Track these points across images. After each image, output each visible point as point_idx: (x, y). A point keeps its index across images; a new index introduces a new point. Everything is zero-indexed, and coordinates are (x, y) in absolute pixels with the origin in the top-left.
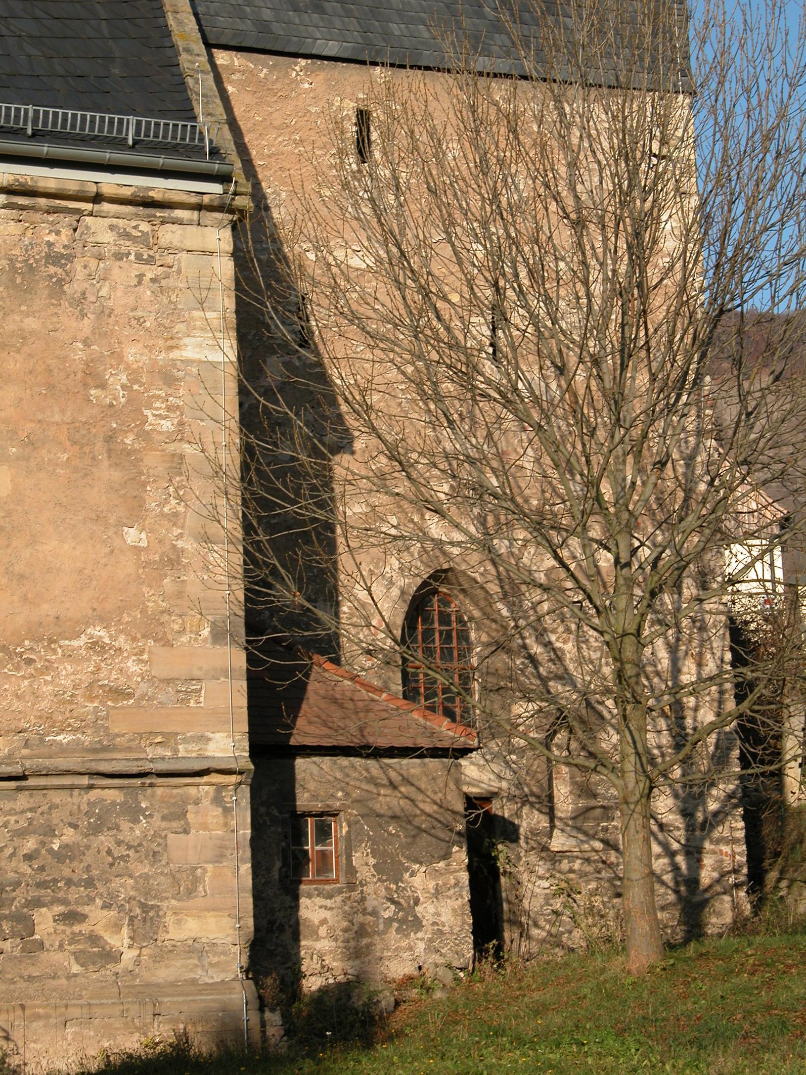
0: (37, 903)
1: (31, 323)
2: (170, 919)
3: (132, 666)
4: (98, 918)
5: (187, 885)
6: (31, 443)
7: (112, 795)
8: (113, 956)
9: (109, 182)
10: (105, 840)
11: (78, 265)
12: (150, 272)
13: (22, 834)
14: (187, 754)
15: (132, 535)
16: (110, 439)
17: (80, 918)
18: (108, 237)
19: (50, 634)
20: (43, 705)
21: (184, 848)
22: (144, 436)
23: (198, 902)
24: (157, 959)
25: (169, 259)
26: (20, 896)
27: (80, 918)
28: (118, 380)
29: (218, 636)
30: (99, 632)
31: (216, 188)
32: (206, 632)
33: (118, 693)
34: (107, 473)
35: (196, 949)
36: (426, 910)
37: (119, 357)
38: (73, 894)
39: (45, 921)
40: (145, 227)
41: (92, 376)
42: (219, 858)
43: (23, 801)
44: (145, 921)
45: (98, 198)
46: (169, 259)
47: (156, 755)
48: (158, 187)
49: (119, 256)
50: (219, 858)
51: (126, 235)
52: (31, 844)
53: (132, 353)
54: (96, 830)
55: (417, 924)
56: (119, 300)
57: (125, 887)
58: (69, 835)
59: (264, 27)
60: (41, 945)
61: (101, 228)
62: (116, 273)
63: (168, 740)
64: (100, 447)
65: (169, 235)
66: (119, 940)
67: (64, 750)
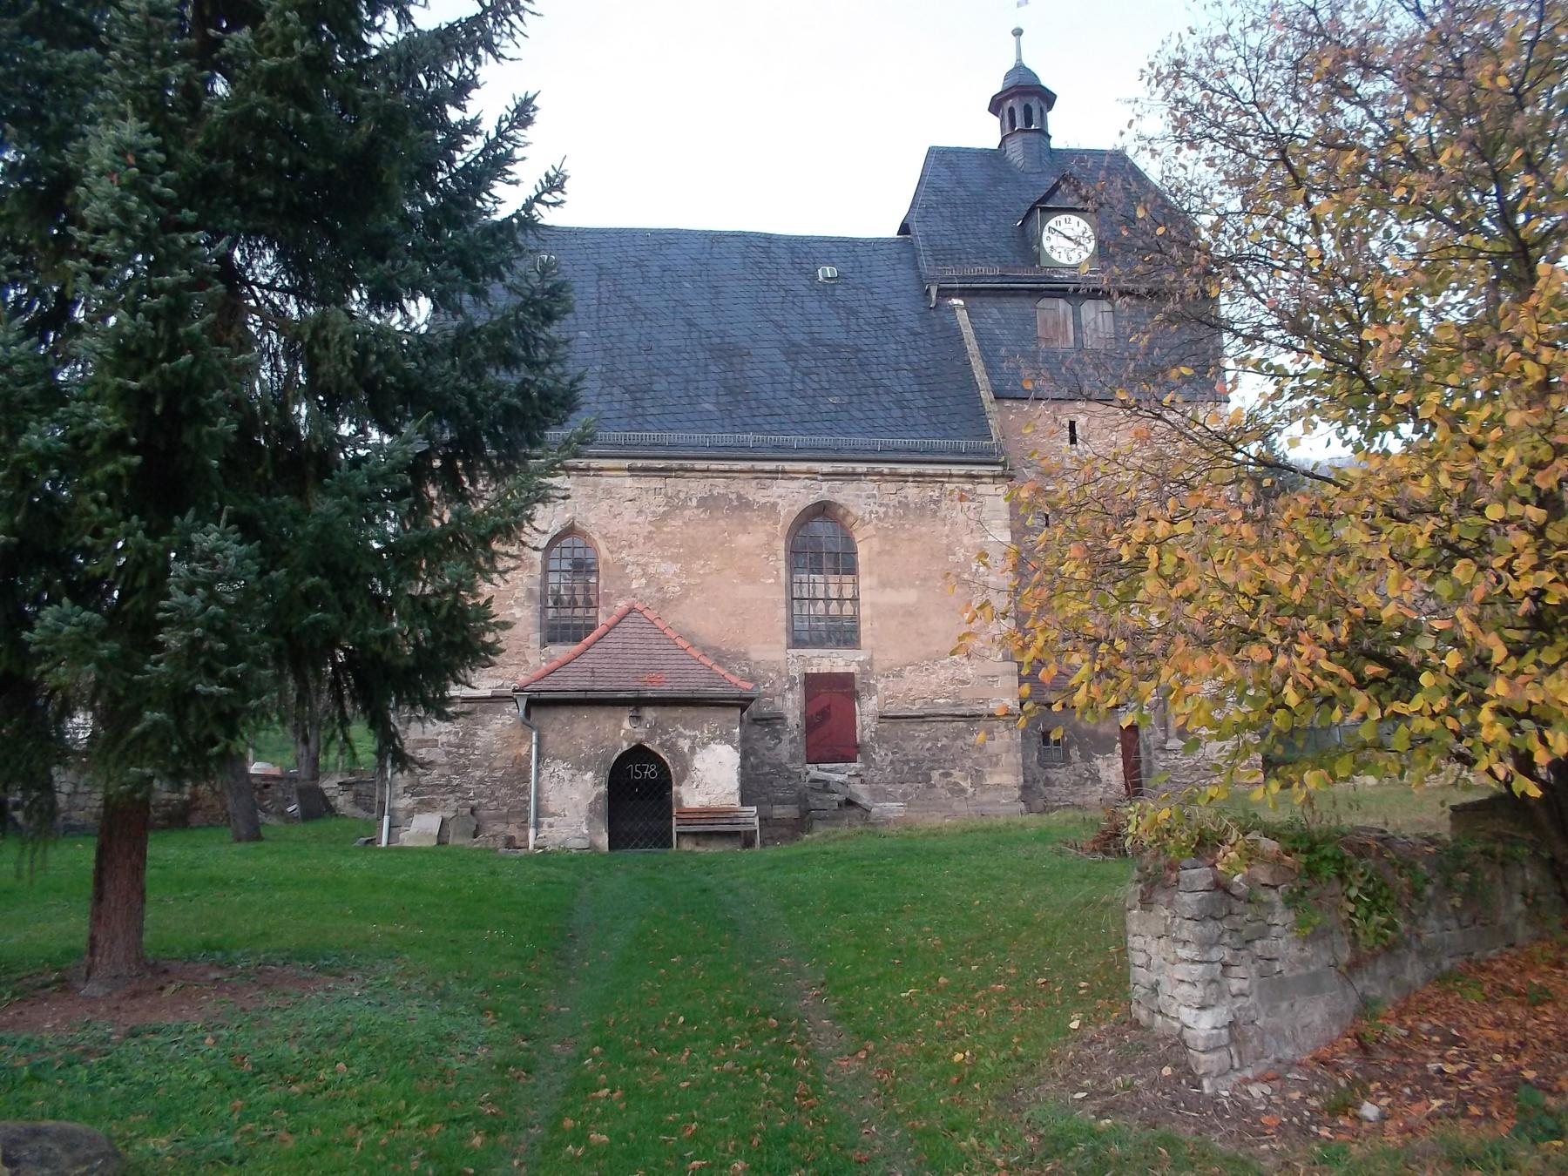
0: (932, 769)
1: (924, 529)
3: (969, 671)
4: (957, 775)
5: (994, 760)
6: (925, 579)
7: (962, 725)
8: (963, 791)
9: (955, 469)
10: (960, 743)
13: (926, 740)
14: (994, 707)
21: (994, 746)
23: (999, 769)
24: (983, 792)
26: (925, 766)
27: (949, 775)
28: (960, 552)
31: (1000, 468)
33: (964, 682)
35: (999, 787)
36: (1103, 774)
37: (960, 541)
39: (936, 775)
41: (950, 550)
44: (977, 777)
45: (951, 475)
47: (978, 709)
48: (976, 470)
50: (1008, 751)
53: (966, 540)
54: (955, 739)
55: (1099, 780)
56: (961, 518)
57: (968, 763)
58: (945, 741)
63: (985, 701)
65: (981, 489)
66: (966, 784)
67: (941, 705)
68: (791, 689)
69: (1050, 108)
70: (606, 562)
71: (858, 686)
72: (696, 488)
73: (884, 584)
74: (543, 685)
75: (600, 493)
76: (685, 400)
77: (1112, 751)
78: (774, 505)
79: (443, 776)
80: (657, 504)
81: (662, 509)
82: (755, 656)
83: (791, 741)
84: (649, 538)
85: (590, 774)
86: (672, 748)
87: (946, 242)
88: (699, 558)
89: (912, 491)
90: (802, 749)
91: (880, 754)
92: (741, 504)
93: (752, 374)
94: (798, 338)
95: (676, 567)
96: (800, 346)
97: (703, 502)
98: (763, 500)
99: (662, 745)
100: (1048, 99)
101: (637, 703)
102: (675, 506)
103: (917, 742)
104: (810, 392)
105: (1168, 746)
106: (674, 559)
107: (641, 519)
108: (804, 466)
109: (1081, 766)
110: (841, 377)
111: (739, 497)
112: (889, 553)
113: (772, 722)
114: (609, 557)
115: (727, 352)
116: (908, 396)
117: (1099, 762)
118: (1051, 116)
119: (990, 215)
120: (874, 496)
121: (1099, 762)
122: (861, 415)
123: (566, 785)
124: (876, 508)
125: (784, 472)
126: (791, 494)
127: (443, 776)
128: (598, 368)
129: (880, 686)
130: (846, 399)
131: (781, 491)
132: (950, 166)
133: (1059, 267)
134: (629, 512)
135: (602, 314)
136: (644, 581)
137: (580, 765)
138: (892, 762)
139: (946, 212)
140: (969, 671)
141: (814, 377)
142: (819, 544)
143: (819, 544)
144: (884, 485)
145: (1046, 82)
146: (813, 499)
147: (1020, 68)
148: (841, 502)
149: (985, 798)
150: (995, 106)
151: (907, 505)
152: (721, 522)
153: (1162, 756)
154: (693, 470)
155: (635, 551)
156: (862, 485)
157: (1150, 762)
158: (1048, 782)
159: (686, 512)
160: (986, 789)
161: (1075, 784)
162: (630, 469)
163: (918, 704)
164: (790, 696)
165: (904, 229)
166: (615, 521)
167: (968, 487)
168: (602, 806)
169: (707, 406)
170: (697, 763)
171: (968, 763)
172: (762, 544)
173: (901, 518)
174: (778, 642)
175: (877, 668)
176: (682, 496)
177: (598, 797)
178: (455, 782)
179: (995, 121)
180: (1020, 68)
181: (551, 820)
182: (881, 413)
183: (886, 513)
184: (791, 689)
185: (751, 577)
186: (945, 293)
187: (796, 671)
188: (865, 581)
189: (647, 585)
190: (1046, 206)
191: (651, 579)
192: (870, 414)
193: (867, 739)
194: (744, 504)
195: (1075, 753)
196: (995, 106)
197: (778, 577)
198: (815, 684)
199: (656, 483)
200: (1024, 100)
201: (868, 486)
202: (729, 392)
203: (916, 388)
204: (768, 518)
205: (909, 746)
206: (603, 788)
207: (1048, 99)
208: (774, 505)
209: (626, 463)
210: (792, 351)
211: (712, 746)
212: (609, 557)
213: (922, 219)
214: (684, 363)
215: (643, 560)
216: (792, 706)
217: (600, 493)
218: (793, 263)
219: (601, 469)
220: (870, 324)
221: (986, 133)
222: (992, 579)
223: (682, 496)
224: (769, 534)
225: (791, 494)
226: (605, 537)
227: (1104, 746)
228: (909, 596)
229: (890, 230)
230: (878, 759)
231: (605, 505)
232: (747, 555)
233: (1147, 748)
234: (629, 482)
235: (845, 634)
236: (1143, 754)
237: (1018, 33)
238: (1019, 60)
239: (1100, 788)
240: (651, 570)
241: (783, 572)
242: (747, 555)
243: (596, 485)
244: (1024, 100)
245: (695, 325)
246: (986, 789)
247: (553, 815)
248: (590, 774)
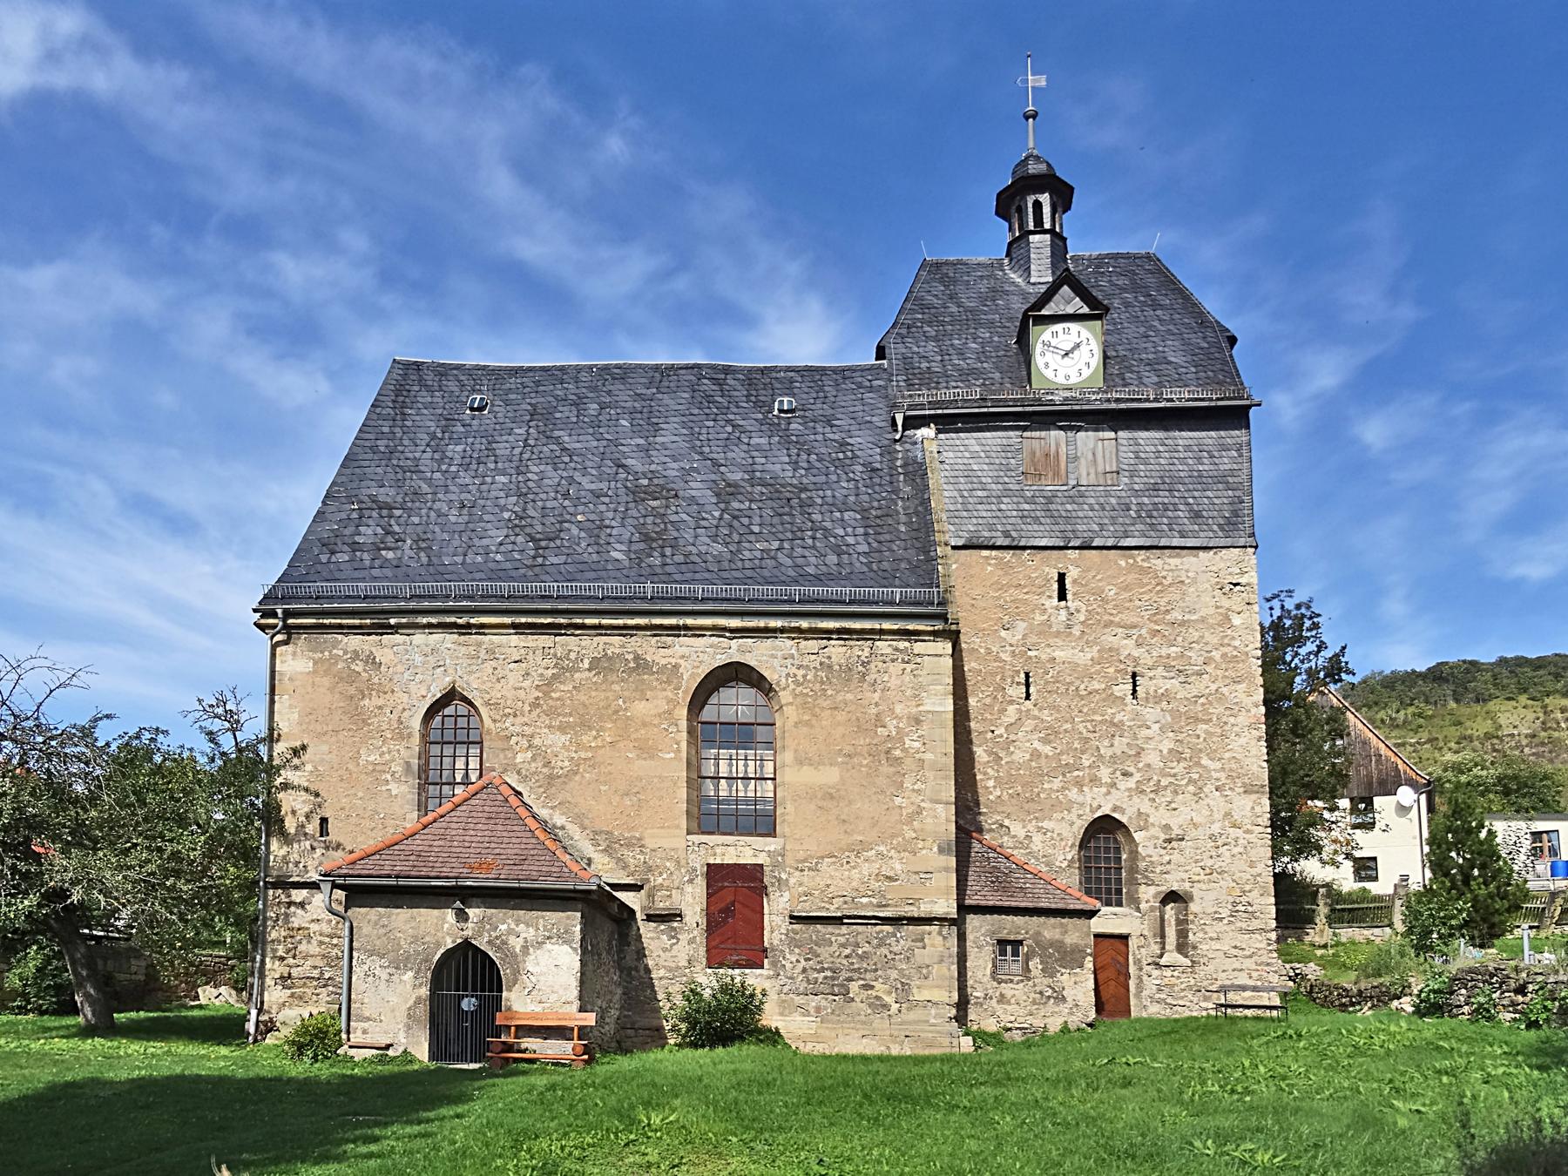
0: (850, 979)
1: (849, 696)
2: (915, 990)
3: (898, 866)
4: (880, 988)
5: (924, 972)
8: (886, 1007)
10: (884, 950)
11: (872, 665)
12: (909, 667)
13: (844, 946)
14: (924, 910)
15: (898, 801)
16: (887, 752)
17: (872, 987)
18: (889, 651)
19: (859, 849)
20: (854, 884)
21: (921, 956)
22: (904, 750)
23: (929, 982)
24: (909, 1009)
25: (919, 660)
26: (845, 975)
27: (872, 987)
28: (892, 725)
29: (941, 850)
30: (882, 848)
32: (935, 849)
33: (889, 878)
34: (886, 769)
37: (892, 710)
38: (868, 976)
39: (854, 987)
40: (907, 644)
41: (879, 721)
42: (941, 961)
43: (844, 929)
46: (919, 660)
49: (893, 661)
51: (896, 649)
52: (847, 952)
53: (898, 709)
54: (879, 946)
55: (1064, 999)
56: (894, 683)
58: (867, 948)
59: (1006, 534)
60: (853, 1000)
61: (883, 646)
62: (891, 669)
63: (914, 902)
64: (883, 756)
65: (919, 647)
66: (889, 999)
67: (864, 906)
68: (691, 881)
69: (1067, 208)
70: (489, 732)
71: (766, 880)
72: (591, 645)
73: (800, 762)
74: (367, 867)
75: (483, 654)
77: (1081, 966)
78: (676, 667)
79: (315, 967)
80: (542, 668)
81: (550, 672)
82: (650, 843)
83: (691, 941)
84: (535, 705)
85: (410, 974)
86: (502, 946)
88: (590, 728)
89: (837, 651)
90: (702, 951)
91: (792, 959)
92: (638, 666)
93: (674, 518)
95: (564, 738)
97: (595, 664)
98: (663, 662)
99: (489, 942)
101: (458, 896)
102: (564, 669)
103: (835, 947)
104: (736, 537)
105: (1163, 961)
106: (562, 729)
107: (527, 684)
109: (1042, 982)
110: (776, 520)
111: (637, 658)
112: (808, 724)
113: (650, 918)
114: (492, 726)
116: (851, 540)
117: (1066, 976)
120: (792, 657)
121: (1065, 978)
122: (789, 562)
123: (383, 985)
124: (794, 670)
125: (686, 627)
126: (698, 655)
127: (315, 967)
128: (506, 515)
129: (792, 881)
130: (776, 544)
131: (685, 650)
134: (514, 675)
135: (526, 456)
136: (529, 754)
137: (400, 964)
138: (804, 970)
140: (898, 866)
141: (745, 521)
142: (725, 709)
143: (725, 709)
144: (803, 643)
146: (721, 660)
148: (752, 663)
149: (912, 1016)
151: (830, 667)
152: (616, 687)
153: (1156, 973)
154: (583, 627)
155: (520, 720)
156: (777, 642)
157: (1140, 978)
158: (1002, 999)
159: (577, 675)
160: (916, 1004)
161: (1034, 1002)
162: (514, 626)
163: (838, 902)
164: (689, 888)
166: (498, 686)
167: (903, 645)
168: (423, 1012)
169: (615, 554)
170: (530, 966)
171: (894, 974)
172: (662, 711)
173: (822, 683)
174: (678, 827)
175: (789, 860)
176: (573, 656)
177: (418, 1000)
178: (327, 976)
181: (366, 1025)
182: (813, 560)
183: (804, 676)
184: (691, 881)
185: (647, 750)
186: (912, 423)
187: (698, 862)
188: (787, 757)
189: (534, 759)
191: (538, 753)
192: (800, 561)
193: (776, 942)
194: (641, 665)
195: (1035, 964)
197: (679, 750)
198: (716, 873)
199: (545, 640)
201: (785, 644)
203: (861, 531)
204: (668, 682)
205: (824, 952)
206: (424, 991)
208: (676, 667)
209: (507, 620)
211: (548, 946)
212: (492, 726)
214: (603, 508)
215: (528, 730)
216: (693, 901)
217: (483, 654)
219: (483, 626)
222: (929, 756)
223: (573, 656)
224: (669, 701)
225: (698, 655)
226: (487, 704)
227: (1070, 958)
228: (830, 776)
230: (788, 966)
231: (489, 665)
232: (644, 724)
233: (1138, 962)
234: (515, 639)
235: (762, 822)
236: (1132, 969)
239: (1064, 1008)
240: (537, 741)
241: (684, 745)
242: (644, 724)
243: (479, 644)
245: (623, 466)
246: (916, 1004)
247: (368, 1019)
248: (410, 974)
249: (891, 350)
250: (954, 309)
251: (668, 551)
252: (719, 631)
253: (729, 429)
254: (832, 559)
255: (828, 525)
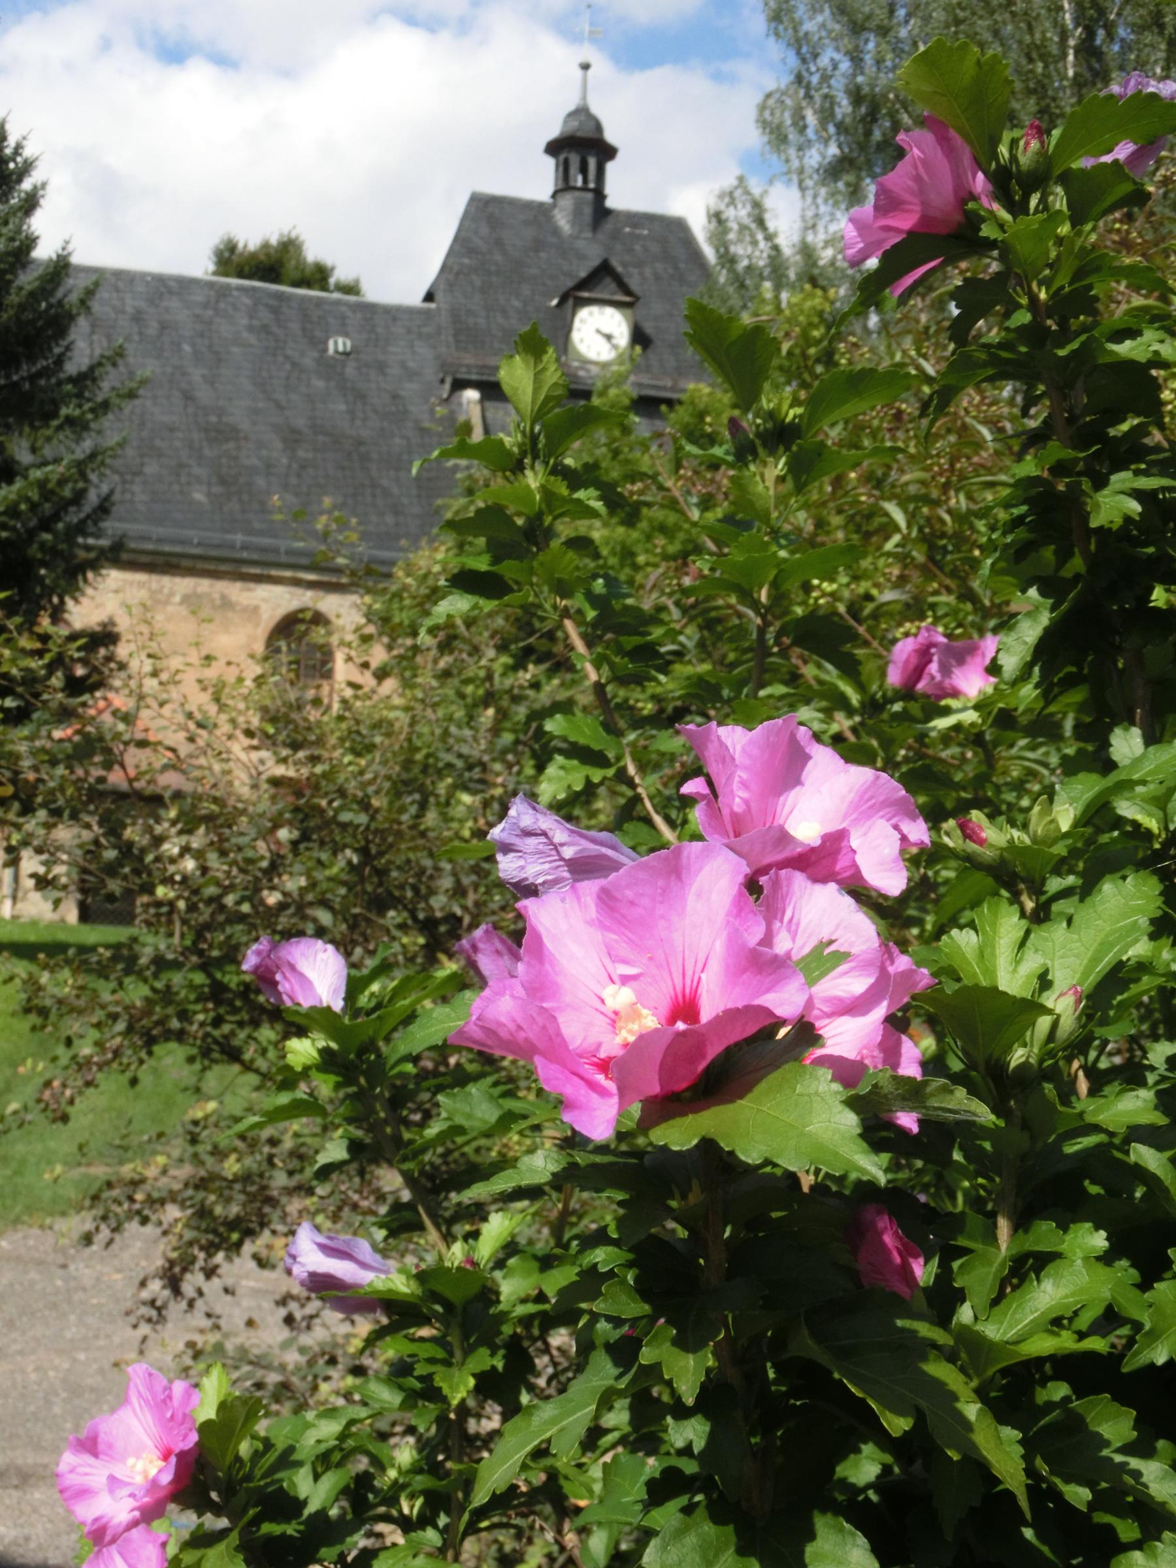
76: (176, 488)
78: (256, 608)
87: (471, 320)
93: (247, 462)
94: (300, 423)
96: (299, 432)
97: (186, 599)
100: (607, 152)
108: (288, 574)
111: (223, 597)
115: (223, 433)
116: (405, 501)
118: (611, 167)
119: (526, 290)
132: (494, 222)
133: (586, 362)
139: (477, 280)
145: (610, 136)
147: (582, 112)
150: (553, 148)
159: (170, 609)
165: (429, 297)
179: (550, 163)
180: (582, 112)
190: (577, 295)
194: (226, 604)
196: (553, 148)
199: (141, 577)
200: (582, 149)
202: (223, 481)
207: (607, 152)
208: (256, 608)
210: (292, 438)
213: (451, 285)
218: (304, 329)
220: (376, 411)
221: (536, 181)
225: (275, 600)
229: (413, 297)
237: (586, 67)
238: (584, 97)
244: (582, 149)
249: (439, 296)
250: (498, 257)
251: (245, 497)
252: (297, 582)
253: (288, 366)
254: (389, 519)
255: (385, 482)
